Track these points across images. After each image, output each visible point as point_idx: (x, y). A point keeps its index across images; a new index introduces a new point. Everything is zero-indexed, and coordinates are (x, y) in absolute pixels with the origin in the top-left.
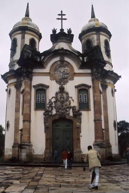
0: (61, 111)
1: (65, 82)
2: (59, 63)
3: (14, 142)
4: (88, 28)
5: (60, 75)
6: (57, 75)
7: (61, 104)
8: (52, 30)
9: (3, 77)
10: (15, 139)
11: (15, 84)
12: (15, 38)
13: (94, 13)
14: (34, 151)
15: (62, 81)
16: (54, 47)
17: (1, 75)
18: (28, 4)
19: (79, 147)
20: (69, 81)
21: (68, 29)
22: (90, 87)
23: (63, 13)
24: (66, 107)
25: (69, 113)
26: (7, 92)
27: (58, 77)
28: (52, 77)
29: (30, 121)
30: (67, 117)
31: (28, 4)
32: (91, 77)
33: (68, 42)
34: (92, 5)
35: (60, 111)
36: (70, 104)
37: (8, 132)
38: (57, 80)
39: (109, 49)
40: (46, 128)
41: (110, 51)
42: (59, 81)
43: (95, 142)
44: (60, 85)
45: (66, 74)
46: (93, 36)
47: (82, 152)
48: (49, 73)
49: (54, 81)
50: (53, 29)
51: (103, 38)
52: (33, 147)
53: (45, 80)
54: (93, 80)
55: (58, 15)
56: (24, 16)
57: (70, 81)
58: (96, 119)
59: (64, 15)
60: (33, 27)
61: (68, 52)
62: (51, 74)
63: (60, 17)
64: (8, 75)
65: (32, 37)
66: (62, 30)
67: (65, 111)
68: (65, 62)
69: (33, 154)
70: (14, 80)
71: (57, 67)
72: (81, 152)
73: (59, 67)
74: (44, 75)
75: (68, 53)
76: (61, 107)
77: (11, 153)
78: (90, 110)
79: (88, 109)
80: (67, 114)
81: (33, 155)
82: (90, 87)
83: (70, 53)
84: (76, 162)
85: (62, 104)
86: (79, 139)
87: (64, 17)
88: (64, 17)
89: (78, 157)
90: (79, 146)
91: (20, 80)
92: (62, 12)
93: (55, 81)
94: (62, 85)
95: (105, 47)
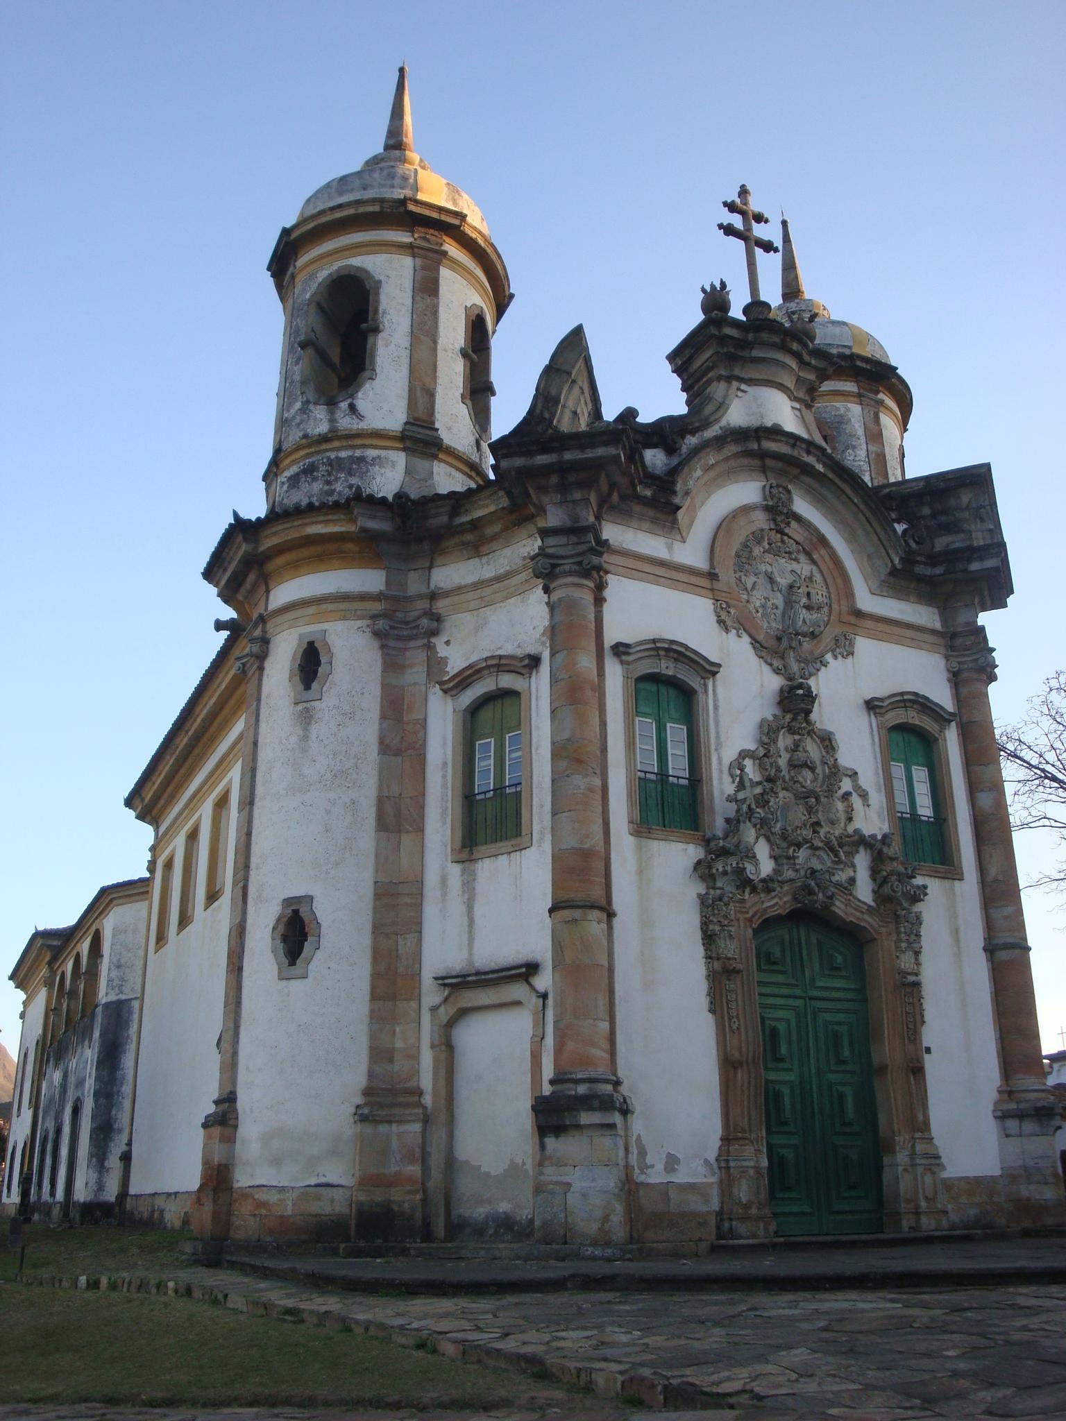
0: (808, 859)
2: (760, 520)
3: (371, 1075)
6: (758, 604)
7: (802, 809)
8: (704, 290)
10: (380, 1054)
11: (377, 607)
14: (642, 1153)
17: (236, 515)
18: (402, 70)
19: (920, 1127)
20: (829, 657)
23: (755, 205)
24: (837, 833)
25: (852, 881)
29: (611, 915)
30: (839, 907)
31: (402, 70)
32: (947, 658)
35: (802, 854)
36: (850, 819)
37: (295, 985)
38: (760, 638)
40: (721, 977)
42: (772, 643)
43: (1008, 1092)
44: (777, 671)
45: (808, 608)
46: (840, 406)
47: (944, 1168)
48: (712, 576)
52: (637, 1125)
53: (688, 620)
54: (956, 679)
55: (725, 204)
56: (376, 145)
58: (1003, 938)
62: (717, 585)
63: (737, 221)
64: (316, 529)
67: (828, 860)
68: (794, 524)
69: (642, 1178)
71: (757, 551)
72: (934, 1160)
73: (765, 551)
74: (674, 584)
75: (820, 467)
76: (807, 833)
77: (339, 1172)
78: (961, 879)
79: (947, 865)
80: (838, 885)
81: (642, 1183)
83: (830, 475)
84: (929, 1240)
85: (810, 810)
86: (917, 1070)
89: (926, 1198)
90: (921, 1118)
92: (744, 192)
93: (746, 639)
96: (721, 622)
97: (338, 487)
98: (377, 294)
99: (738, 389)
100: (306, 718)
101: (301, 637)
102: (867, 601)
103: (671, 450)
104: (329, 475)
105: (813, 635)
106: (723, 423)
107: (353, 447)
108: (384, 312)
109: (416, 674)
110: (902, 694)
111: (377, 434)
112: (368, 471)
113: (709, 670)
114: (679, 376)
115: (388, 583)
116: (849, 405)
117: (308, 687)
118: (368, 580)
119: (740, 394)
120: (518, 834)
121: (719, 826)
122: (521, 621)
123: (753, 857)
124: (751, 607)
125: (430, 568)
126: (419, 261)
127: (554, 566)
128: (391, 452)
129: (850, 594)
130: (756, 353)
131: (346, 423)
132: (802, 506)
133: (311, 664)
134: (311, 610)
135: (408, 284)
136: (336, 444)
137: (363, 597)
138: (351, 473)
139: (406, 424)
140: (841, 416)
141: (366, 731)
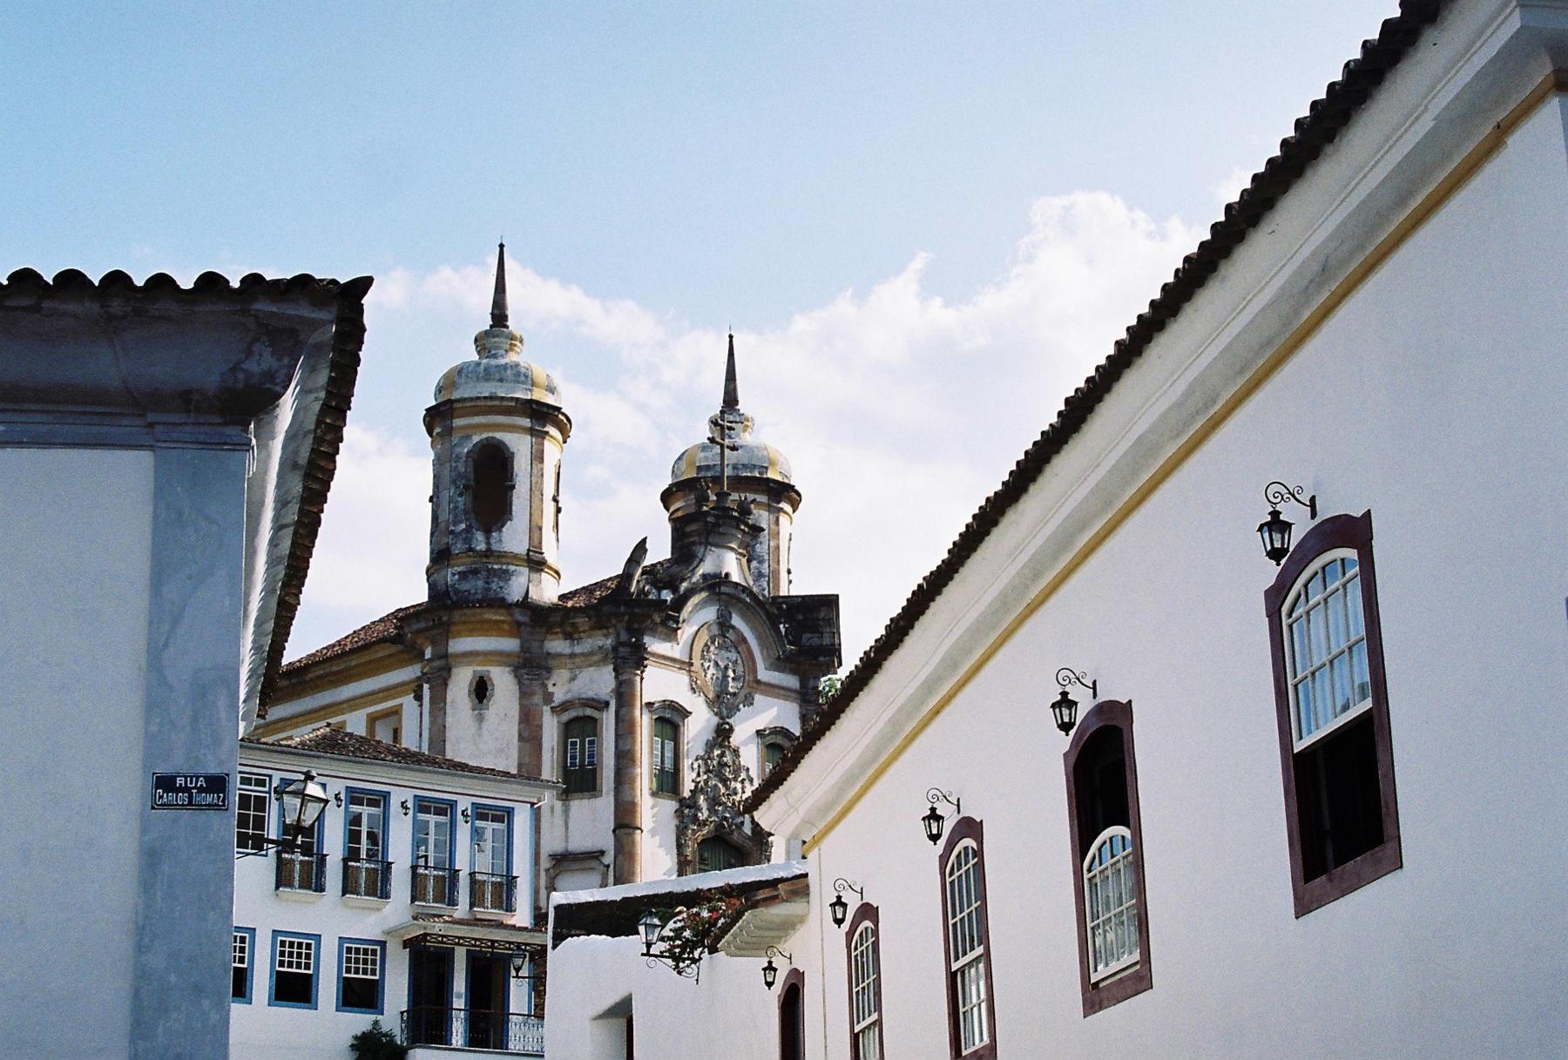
93: (702, 698)
97: (494, 586)
100: (480, 719)
102: (764, 674)
103: (675, 590)
109: (538, 699)
111: (516, 557)
113: (686, 714)
117: (481, 701)
118: (510, 644)
120: (594, 789)
121: (686, 794)
122: (601, 682)
123: (700, 810)
129: (755, 671)
132: (736, 621)
133: (481, 690)
137: (508, 655)
141: (512, 728)
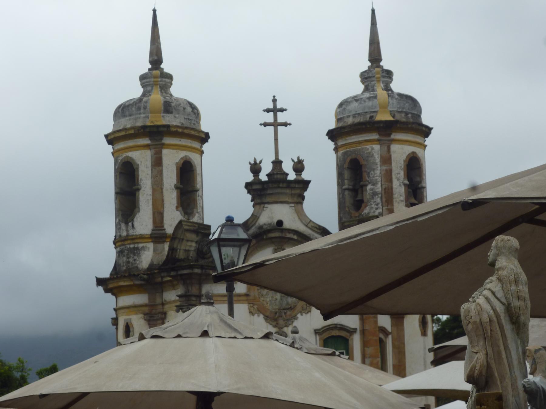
1: (288, 320)
4: (354, 116)
5: (276, 299)
6: (268, 300)
8: (250, 163)
9: (100, 282)
11: (146, 309)
12: (131, 158)
13: (378, 43)
15: (281, 316)
16: (254, 217)
17: (96, 278)
18: (154, 11)
21: (296, 160)
22: (352, 331)
23: (279, 106)
26: (115, 327)
27: (269, 306)
28: (255, 307)
31: (154, 11)
33: (295, 199)
34: (373, 11)
39: (420, 182)
41: (424, 188)
44: (275, 327)
48: (247, 295)
49: (259, 316)
50: (252, 162)
51: (400, 152)
55: (264, 111)
57: (302, 315)
59: (282, 110)
60: (183, 121)
61: (294, 234)
63: (270, 117)
65: (182, 154)
66: (277, 163)
70: (140, 299)
75: (295, 237)
82: (355, 330)
83: (300, 239)
87: (282, 117)
88: (282, 117)
91: (158, 301)
92: (274, 101)
93: (262, 316)
94: (282, 328)
95: (405, 185)
96: (250, 312)
97: (131, 260)
98: (138, 171)
99: (264, 207)
101: (125, 320)
104: (128, 254)
105: (291, 308)
106: (257, 224)
107: (134, 243)
108: (141, 180)
110: (329, 325)
112: (140, 253)
114: (250, 194)
115: (149, 299)
116: (374, 146)
119: (265, 209)
124: (265, 303)
125: (162, 292)
126: (153, 151)
127: (182, 309)
128: (147, 244)
130: (269, 192)
131: (131, 232)
134: (126, 310)
135: (149, 163)
136: (129, 242)
138: (134, 254)
139: (153, 230)
140: (369, 153)
